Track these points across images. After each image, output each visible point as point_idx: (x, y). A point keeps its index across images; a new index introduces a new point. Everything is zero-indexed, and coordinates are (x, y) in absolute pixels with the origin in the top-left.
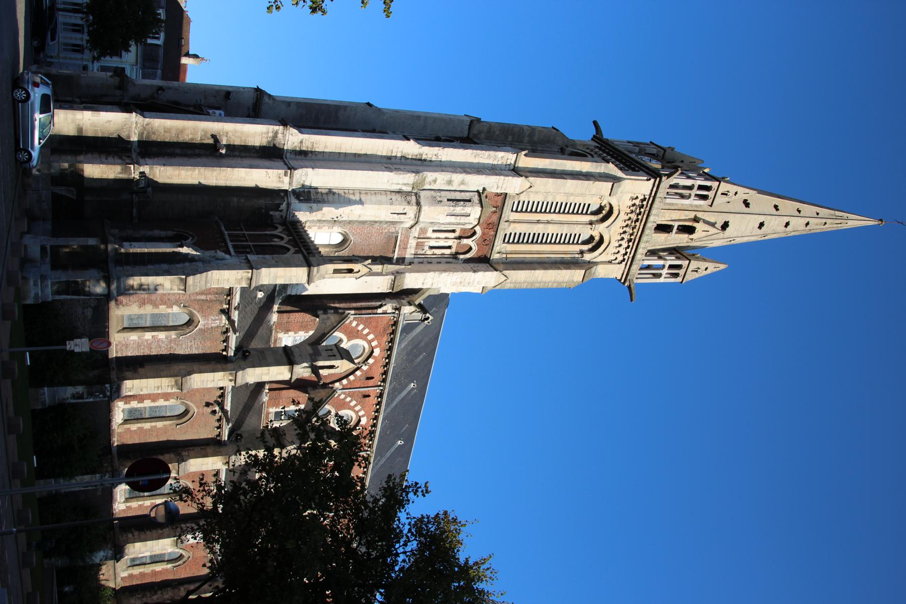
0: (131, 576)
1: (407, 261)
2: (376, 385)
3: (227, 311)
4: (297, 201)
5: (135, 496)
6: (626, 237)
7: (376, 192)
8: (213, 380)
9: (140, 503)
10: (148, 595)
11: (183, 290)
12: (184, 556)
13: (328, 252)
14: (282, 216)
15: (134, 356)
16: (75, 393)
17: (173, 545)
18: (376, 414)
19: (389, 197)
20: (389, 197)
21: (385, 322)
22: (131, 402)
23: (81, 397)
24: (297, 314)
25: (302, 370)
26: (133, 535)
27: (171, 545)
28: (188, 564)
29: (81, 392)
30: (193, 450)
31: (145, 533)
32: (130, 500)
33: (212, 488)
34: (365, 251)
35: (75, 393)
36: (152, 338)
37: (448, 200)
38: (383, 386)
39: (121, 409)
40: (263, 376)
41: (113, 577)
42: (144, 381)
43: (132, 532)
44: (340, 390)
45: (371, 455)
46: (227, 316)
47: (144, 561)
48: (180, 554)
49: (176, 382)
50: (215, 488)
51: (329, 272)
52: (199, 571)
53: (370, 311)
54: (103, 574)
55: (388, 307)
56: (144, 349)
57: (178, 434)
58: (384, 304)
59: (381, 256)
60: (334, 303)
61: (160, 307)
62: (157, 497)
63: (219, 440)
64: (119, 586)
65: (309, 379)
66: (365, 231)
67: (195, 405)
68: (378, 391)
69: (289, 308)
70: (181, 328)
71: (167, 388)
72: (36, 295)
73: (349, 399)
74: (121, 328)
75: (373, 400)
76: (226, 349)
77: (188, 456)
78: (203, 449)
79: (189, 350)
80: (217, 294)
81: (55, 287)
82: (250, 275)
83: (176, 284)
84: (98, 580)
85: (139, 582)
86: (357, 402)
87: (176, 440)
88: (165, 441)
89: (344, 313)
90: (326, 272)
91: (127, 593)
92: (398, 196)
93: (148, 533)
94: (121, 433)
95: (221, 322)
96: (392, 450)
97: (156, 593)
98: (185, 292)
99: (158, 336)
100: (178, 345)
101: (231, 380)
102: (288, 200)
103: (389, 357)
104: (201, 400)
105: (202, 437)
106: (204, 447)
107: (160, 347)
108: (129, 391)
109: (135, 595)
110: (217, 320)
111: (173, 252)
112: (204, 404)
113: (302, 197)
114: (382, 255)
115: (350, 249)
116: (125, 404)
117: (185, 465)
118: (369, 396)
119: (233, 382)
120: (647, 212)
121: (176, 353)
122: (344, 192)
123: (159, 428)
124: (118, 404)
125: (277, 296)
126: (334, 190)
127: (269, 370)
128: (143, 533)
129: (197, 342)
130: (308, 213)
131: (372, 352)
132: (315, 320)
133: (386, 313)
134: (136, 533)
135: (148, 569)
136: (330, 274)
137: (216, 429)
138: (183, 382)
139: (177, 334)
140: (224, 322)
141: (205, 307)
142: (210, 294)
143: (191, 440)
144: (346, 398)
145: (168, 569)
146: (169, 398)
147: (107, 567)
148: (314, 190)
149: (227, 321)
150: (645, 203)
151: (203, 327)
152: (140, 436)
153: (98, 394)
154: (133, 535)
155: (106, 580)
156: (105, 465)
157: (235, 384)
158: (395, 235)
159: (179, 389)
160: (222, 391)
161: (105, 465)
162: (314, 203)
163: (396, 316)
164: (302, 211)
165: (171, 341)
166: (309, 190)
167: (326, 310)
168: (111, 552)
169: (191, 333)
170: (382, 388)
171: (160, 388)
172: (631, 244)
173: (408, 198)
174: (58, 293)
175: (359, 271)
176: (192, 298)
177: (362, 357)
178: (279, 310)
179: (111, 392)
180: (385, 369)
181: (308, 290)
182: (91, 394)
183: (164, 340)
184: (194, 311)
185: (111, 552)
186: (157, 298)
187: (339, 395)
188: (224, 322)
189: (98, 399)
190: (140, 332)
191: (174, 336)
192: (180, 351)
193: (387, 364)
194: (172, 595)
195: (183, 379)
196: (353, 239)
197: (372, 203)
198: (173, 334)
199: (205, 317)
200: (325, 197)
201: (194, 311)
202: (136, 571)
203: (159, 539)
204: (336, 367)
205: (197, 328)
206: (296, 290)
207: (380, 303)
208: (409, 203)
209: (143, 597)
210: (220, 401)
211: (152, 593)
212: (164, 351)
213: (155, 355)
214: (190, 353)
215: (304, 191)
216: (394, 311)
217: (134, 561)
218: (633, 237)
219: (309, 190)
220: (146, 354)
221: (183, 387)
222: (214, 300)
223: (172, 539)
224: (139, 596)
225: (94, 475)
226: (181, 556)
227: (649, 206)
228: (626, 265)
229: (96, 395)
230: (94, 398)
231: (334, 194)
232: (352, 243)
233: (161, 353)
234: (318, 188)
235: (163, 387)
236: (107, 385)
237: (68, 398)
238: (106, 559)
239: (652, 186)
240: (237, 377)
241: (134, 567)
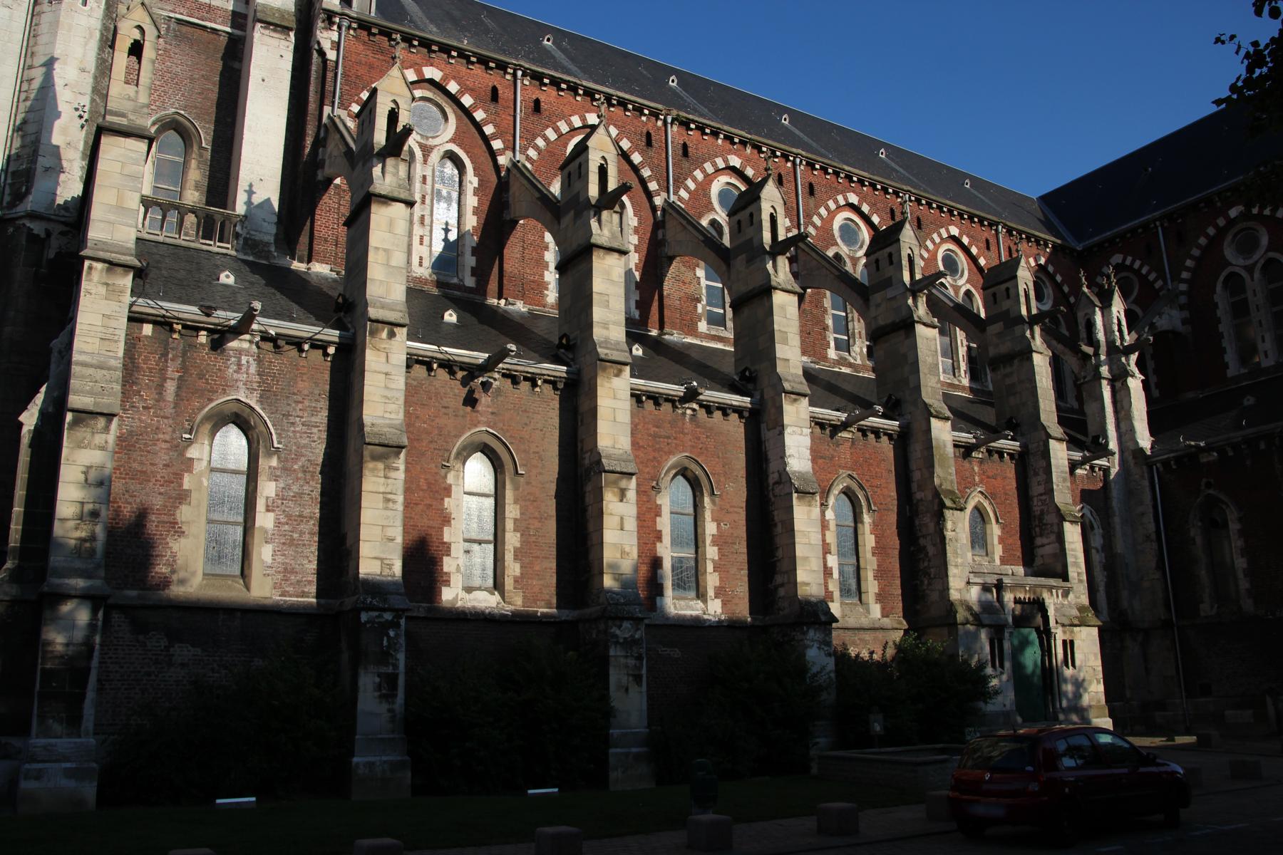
0: (880, 598)
1: (241, 9)
2: (511, 83)
3: (216, 336)
4: (30, 198)
5: (693, 579)
7: (32, 35)
8: (386, 374)
9: (710, 567)
10: (926, 564)
11: (110, 422)
12: (848, 488)
13: (199, 162)
14: (62, 233)
15: (319, 556)
16: (377, 694)
17: (809, 502)
18: (581, 92)
21: (362, 47)
22: (446, 569)
23: (391, 680)
24: (318, 223)
25: (389, 178)
26: (782, 585)
27: (810, 506)
28: (867, 480)
29: (377, 680)
30: (582, 441)
31: (779, 560)
32: (701, 590)
33: (689, 412)
34: (208, 89)
35: (377, 694)
36: (273, 511)
38: (515, 70)
39: (462, 594)
40: (394, 263)
41: (880, 635)
42: (364, 532)
43: (776, 588)
44: (514, 156)
45: (675, 112)
46: (228, 335)
47: (850, 570)
48: (843, 496)
49: (375, 458)
50: (687, 405)
51: (132, 94)
52: (884, 460)
53: (330, 75)
54: (872, 653)
55: (326, 38)
56: (302, 533)
57: (540, 474)
58: (316, 47)
59: (223, 58)
60: (304, 147)
61: (186, 487)
62: (699, 530)
63: (565, 384)
64: (900, 623)
65: (484, 216)
66: (158, 83)
67: (469, 428)
68: (526, 82)
69: (304, 239)
70: (255, 445)
71: (390, 481)
72: (69, 774)
73: (540, 142)
74: (241, 581)
75: (548, 95)
76: (321, 346)
77: (591, 451)
78: (582, 421)
79: (315, 430)
80: (165, 355)
81: (57, 728)
82: (99, 266)
83: (89, 436)
84: (882, 665)
85: (898, 582)
86: (548, 127)
87: (558, 479)
88: (558, 504)
89: (325, 124)
90: (129, 99)
91: (918, 607)
93: (780, 553)
94: (525, 597)
95: (247, 352)
96: (684, 94)
97: (923, 549)
98: (114, 415)
99: (267, 498)
100: (299, 456)
101: (392, 335)
102: (21, 218)
103: (446, 49)
104: (456, 416)
105: (556, 421)
106: (579, 418)
107: (300, 495)
108: (390, 569)
109: (924, 590)
110: (240, 360)
111: (31, 445)
112: (469, 409)
113: (21, 188)
114: (221, 55)
115: (198, 117)
116: (449, 585)
117: (609, 457)
118: (537, 102)
119: (396, 330)
121: (320, 460)
122: (24, 101)
123: (521, 514)
124: (447, 601)
125: (267, 258)
126: (18, 122)
127: (377, 248)
128: (778, 564)
129: (295, 409)
130: (62, 177)
131: (431, 82)
132: (337, 186)
133: (339, 43)
134: (779, 579)
135: (870, 563)
136: (137, 92)
137: (537, 389)
138: (377, 442)
139: (270, 453)
140: (246, 345)
141: (201, 384)
142: (163, 371)
143: (560, 446)
144: (536, 148)
145: (874, 522)
146: (443, 486)
147: (854, 643)
148: (11, 163)
149: (242, 337)
151: (256, 395)
152: (538, 557)
153: (385, 639)
154: (782, 585)
155: (885, 647)
156: (594, 636)
157: (402, 326)
158: (173, 25)
159: (400, 453)
160: (435, 366)
161: (594, 636)
162: (36, 163)
163: (345, 23)
164: (56, 189)
165: (284, 469)
166: (9, 175)
167: (316, 163)
168: (811, 633)
169: (268, 421)
170: (519, 73)
171: (390, 496)
174: (74, 721)
175: (139, 27)
176: (169, 410)
177: (444, 104)
178: (306, 259)
179: (384, 610)
180: (473, 59)
181: (268, 200)
182: (385, 656)
183: (282, 485)
184: (207, 409)
185: (811, 633)
186: (160, 494)
187: (529, 158)
188: (246, 345)
189: (402, 641)
190: (253, 537)
191: (274, 462)
192: (317, 451)
193: (462, 54)
194: (929, 515)
195: (367, 440)
196: (174, 110)
197: (52, 43)
198: (268, 463)
199: (227, 386)
201: (207, 409)
202: (871, 586)
203: (793, 530)
204: (394, 106)
205: (258, 408)
206: (266, 224)
207: (315, 55)
209: (930, 575)
210: (465, 373)
211: (922, 556)
212: (314, 488)
213: (321, 509)
214: (324, 427)
216: (335, 27)
217: (849, 591)
219: (9, 175)
220: (317, 528)
221: (391, 443)
222: (184, 362)
223: (795, 502)
224: (926, 582)
225: (612, 659)
226: (847, 492)
229: (389, 646)
230: (396, 650)
231: (24, 122)
232: (182, 112)
233: (317, 494)
234: (9, 156)
235: (388, 490)
236: (364, 617)
237: (390, 711)
238: (829, 644)
240: (380, 318)
241: (863, 590)
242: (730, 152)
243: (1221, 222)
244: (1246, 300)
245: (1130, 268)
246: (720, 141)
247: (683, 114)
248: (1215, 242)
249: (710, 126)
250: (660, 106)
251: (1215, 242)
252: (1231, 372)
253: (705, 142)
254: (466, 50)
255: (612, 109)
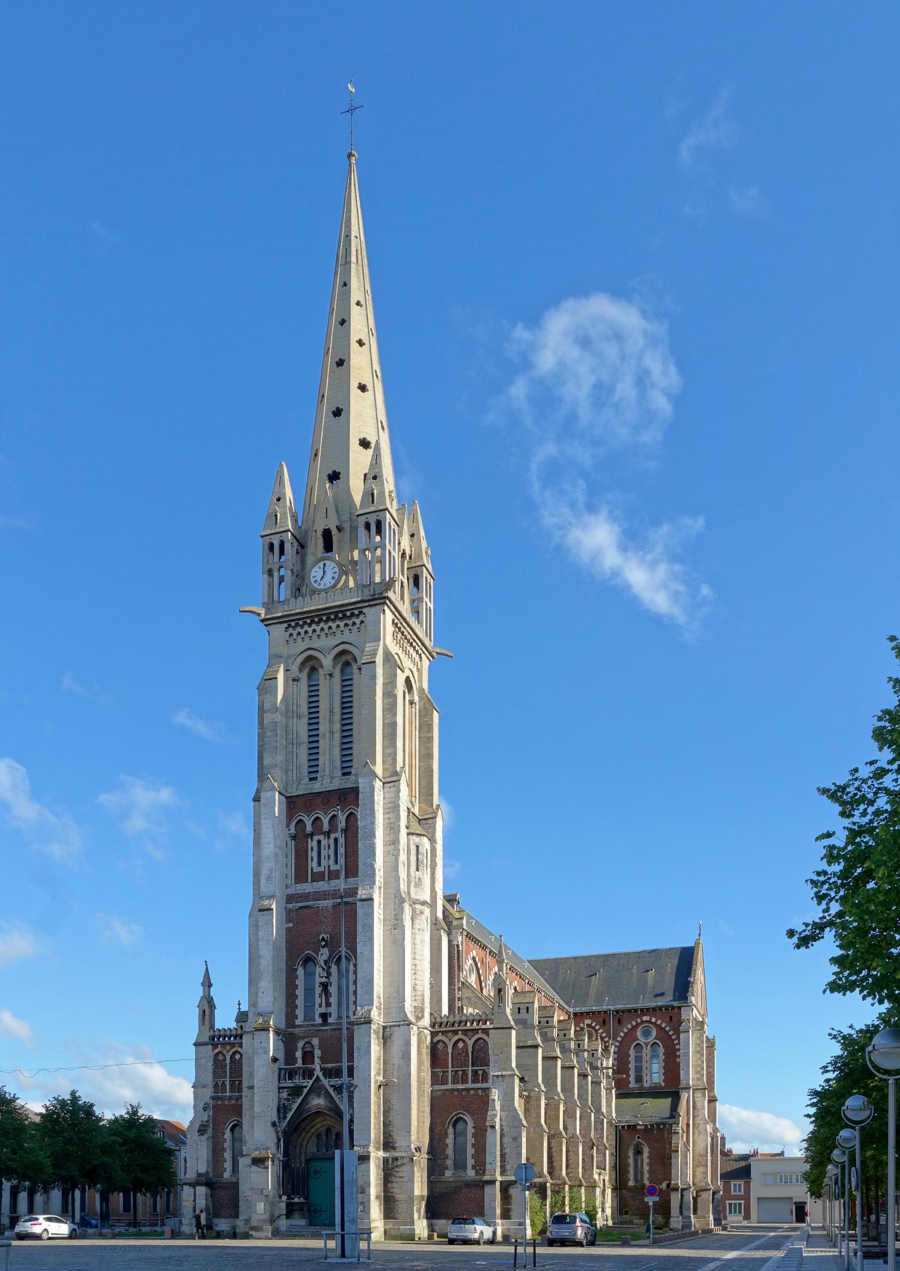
4: (423, 1020)
19: (417, 931)
20: (417, 931)
37: (418, 870)
92: (417, 922)
173: (418, 912)
200: (419, 993)
208: (422, 913)
215: (415, 1012)
227: (399, 617)
243: (639, 1021)
244: (642, 1056)
245: (594, 1028)
248: (635, 1028)
251: (635, 1028)
252: (630, 1086)
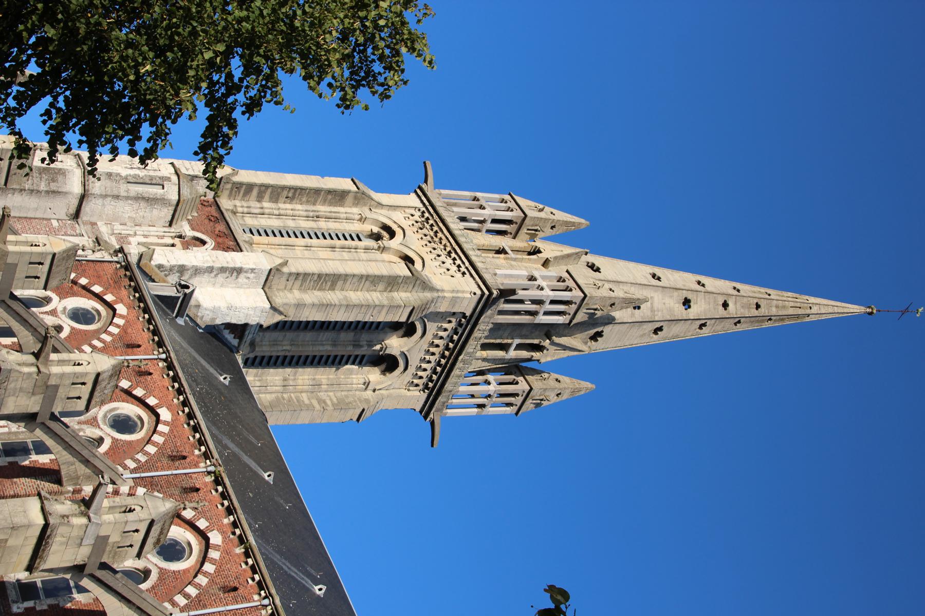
6: (443, 254)
45: (221, 469)
120: (438, 220)
150: (427, 215)
172: (453, 255)
218: (448, 249)
228: (471, 275)
239: (418, 199)
242: (223, 533)
246: (226, 521)
247: (224, 475)
249: (231, 500)
250: (216, 455)
253: (215, 508)
254: (154, 320)
255: (186, 426)
